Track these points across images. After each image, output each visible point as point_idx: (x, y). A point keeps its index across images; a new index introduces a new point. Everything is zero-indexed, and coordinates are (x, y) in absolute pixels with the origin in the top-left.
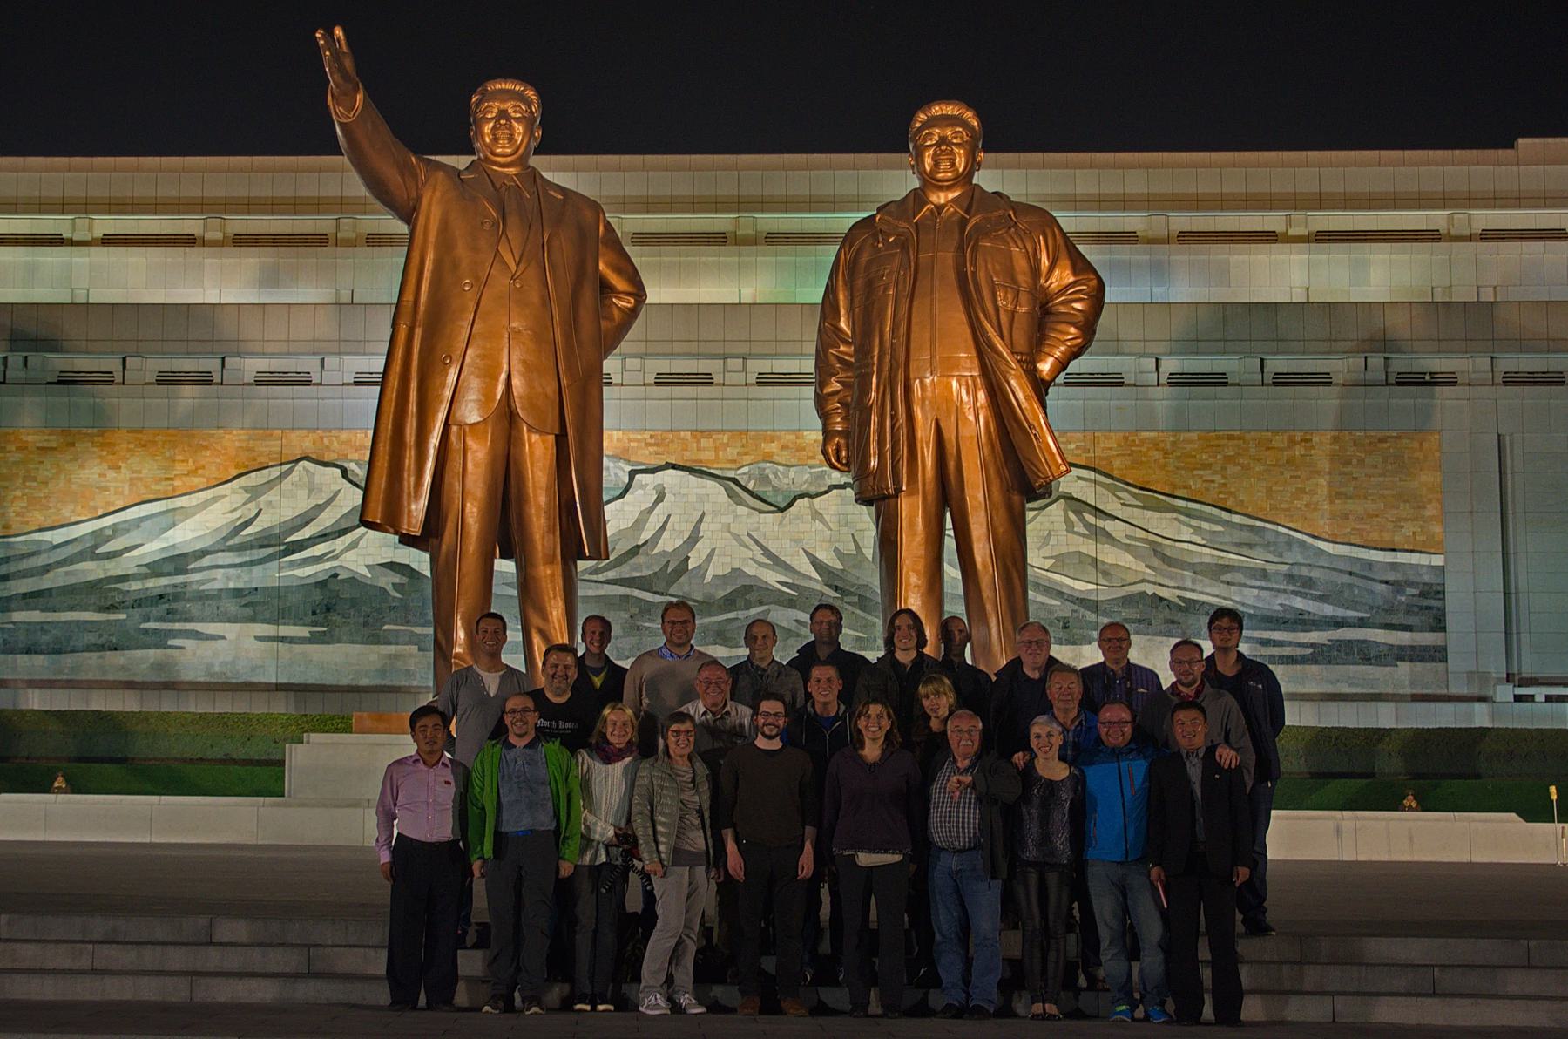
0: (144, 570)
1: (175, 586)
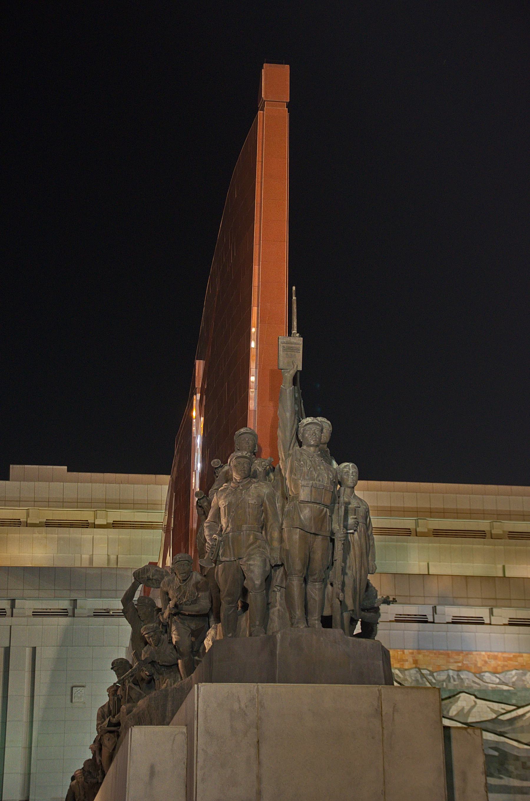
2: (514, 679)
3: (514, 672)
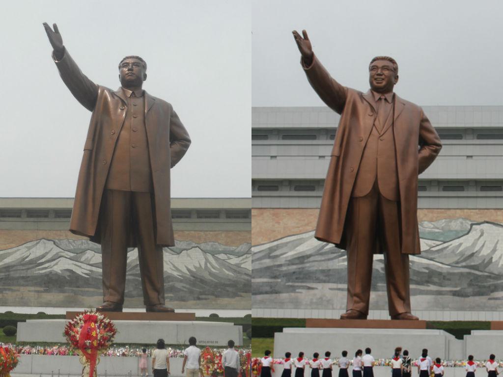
0: (287, 262)
1: (299, 268)
2: (443, 225)
3: (443, 221)
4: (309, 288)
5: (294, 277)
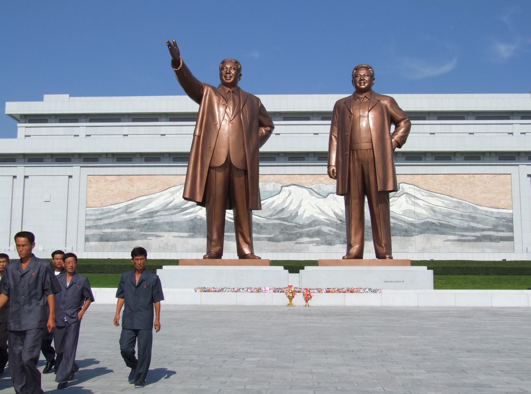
4: (158, 236)
5: (146, 228)
